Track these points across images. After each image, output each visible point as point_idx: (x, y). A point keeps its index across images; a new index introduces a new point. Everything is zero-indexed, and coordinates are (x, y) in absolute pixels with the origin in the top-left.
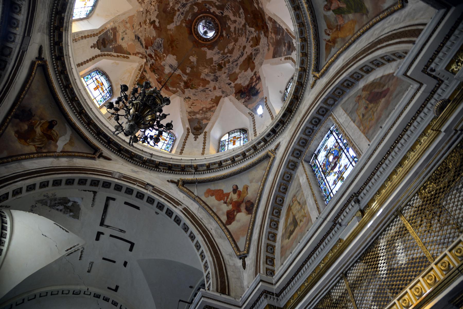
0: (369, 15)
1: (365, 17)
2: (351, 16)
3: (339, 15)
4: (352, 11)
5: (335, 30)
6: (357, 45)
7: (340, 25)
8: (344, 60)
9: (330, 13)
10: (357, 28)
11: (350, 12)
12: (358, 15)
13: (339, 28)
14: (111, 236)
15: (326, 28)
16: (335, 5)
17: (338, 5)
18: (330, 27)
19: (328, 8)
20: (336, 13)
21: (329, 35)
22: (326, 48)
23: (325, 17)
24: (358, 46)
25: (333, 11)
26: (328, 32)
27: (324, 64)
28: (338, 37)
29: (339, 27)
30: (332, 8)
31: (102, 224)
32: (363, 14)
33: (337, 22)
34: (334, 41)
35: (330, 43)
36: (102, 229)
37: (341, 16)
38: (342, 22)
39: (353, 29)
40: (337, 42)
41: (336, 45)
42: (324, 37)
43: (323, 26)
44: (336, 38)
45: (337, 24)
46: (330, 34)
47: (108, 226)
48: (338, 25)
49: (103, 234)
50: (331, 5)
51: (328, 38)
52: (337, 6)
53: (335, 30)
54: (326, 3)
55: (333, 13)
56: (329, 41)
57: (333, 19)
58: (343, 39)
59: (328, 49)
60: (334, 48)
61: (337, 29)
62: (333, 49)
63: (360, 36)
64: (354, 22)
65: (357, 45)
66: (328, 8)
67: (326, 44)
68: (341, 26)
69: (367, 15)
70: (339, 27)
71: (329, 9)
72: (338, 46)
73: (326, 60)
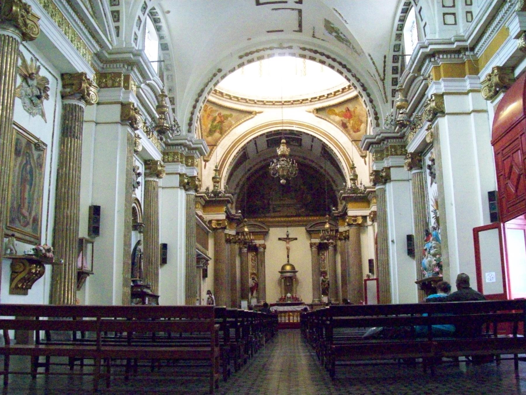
2: (209, 126)
12: (208, 130)
13: (208, 117)
14: (286, 2)
16: (218, 119)
18: (212, 111)
23: (218, 111)
25: (216, 117)
31: (300, 11)
36: (299, 6)
42: (210, 106)
43: (215, 108)
47: (293, 9)
49: (296, 2)
51: (209, 108)
71: (218, 114)
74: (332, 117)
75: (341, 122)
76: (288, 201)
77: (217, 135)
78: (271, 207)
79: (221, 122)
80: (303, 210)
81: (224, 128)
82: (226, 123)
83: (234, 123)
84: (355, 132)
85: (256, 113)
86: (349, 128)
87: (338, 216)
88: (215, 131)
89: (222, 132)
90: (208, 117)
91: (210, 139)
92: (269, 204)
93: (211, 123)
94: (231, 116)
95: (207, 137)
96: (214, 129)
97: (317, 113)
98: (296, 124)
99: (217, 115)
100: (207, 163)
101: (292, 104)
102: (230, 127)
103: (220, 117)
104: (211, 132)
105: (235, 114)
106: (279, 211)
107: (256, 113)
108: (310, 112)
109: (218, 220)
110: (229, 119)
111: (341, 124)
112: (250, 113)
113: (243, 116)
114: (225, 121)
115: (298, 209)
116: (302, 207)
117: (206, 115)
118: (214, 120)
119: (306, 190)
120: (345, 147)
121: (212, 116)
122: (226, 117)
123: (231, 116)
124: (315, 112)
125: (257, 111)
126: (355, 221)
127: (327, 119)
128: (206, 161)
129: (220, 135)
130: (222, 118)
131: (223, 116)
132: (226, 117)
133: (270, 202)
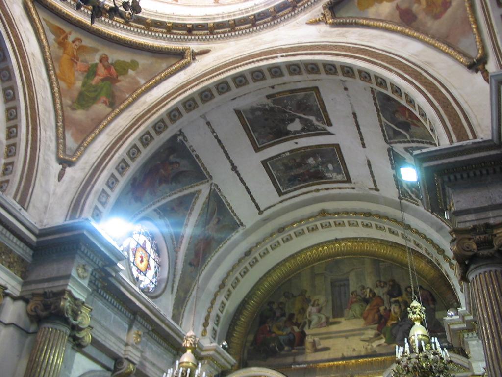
0: (68, 108)
1: (69, 102)
2: (79, 84)
3: (89, 69)
4: (84, 89)
5: (75, 53)
6: (43, 80)
7: (77, 63)
8: (33, 54)
9: (96, 60)
10: (63, 85)
11: (83, 85)
12: (76, 94)
13: (74, 60)
15: (84, 43)
16: (102, 71)
17: (99, 75)
18: (82, 49)
19: (104, 59)
20: (92, 65)
21: (73, 42)
22: (59, 28)
23: (96, 50)
24: (41, 81)
25: (96, 65)
26: (77, 43)
27: (40, 16)
28: (64, 53)
29: (75, 60)
30: (100, 65)
32: (73, 102)
33: (82, 61)
34: (62, 44)
35: (64, 39)
37: (86, 71)
38: (78, 67)
39: (64, 80)
40: (58, 47)
41: (56, 45)
43: (87, 42)
44: (65, 49)
45: (80, 60)
46: (73, 45)
48: (78, 60)
50: (104, 66)
51: (71, 38)
52: (99, 72)
53: (75, 53)
54: (110, 61)
55: (94, 63)
56: (66, 37)
57: (88, 58)
58: (58, 59)
59: (57, 31)
60: (55, 40)
61: (74, 57)
62: (52, 37)
63: (52, 89)
64: (70, 85)
65: (43, 80)
66: (104, 59)
67: (64, 32)
68: (75, 65)
69: (70, 106)
70: (75, 60)
71: (101, 61)
72: (54, 46)
73: (44, 19)
74: (372, 12)
75: (397, 12)
76: (345, 325)
77: (100, 108)
78: (309, 340)
79: (111, 79)
80: (383, 341)
81: (117, 93)
82: (123, 83)
83: (142, 82)
84: (437, 17)
85: (195, 55)
86: (421, 16)
87: (461, 330)
88: (95, 100)
89: (115, 103)
90: (74, 60)
91: (79, 115)
92: (303, 335)
93: (81, 77)
94: (134, 65)
95: (73, 109)
96: (93, 95)
97: (334, 16)
98: (282, 50)
99: (97, 61)
100: (68, 170)
101: (274, 18)
102: (135, 91)
103: (108, 68)
104: (84, 100)
105: (143, 61)
106: (326, 349)
107: (195, 55)
108: (316, 22)
109: (45, 295)
110: (131, 72)
111: (397, 19)
112: (180, 54)
113: (164, 65)
114: (119, 78)
115: (370, 340)
116: (377, 336)
117: (66, 57)
118: (92, 71)
119: (386, 298)
120: (418, 63)
121: (85, 61)
122: (123, 68)
123: (134, 65)
124: (328, 14)
125: (196, 51)
126: (488, 243)
127: (361, 21)
128: (66, 163)
129: (109, 110)
130: (113, 70)
131: (117, 64)
132: (123, 68)
133: (307, 331)
